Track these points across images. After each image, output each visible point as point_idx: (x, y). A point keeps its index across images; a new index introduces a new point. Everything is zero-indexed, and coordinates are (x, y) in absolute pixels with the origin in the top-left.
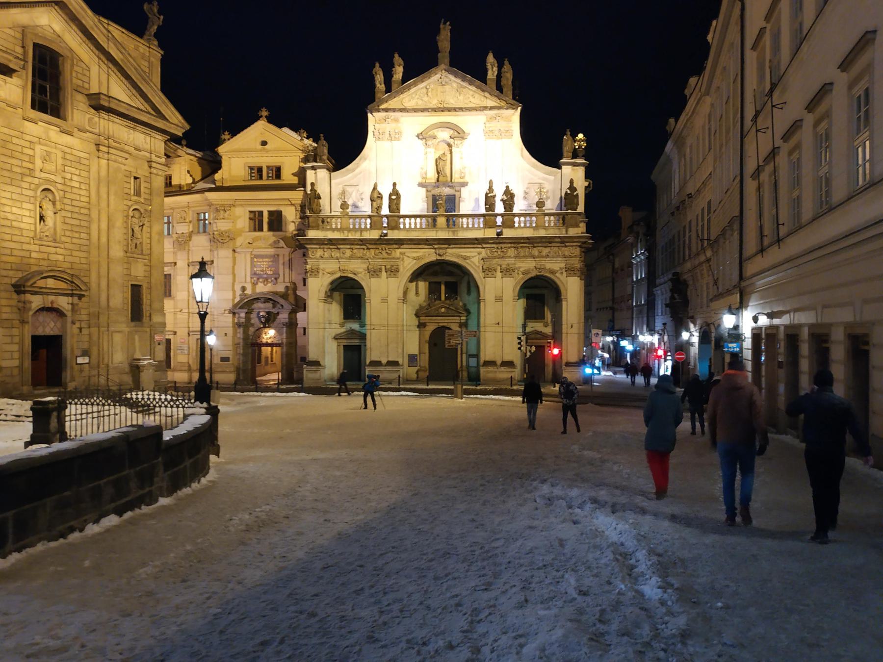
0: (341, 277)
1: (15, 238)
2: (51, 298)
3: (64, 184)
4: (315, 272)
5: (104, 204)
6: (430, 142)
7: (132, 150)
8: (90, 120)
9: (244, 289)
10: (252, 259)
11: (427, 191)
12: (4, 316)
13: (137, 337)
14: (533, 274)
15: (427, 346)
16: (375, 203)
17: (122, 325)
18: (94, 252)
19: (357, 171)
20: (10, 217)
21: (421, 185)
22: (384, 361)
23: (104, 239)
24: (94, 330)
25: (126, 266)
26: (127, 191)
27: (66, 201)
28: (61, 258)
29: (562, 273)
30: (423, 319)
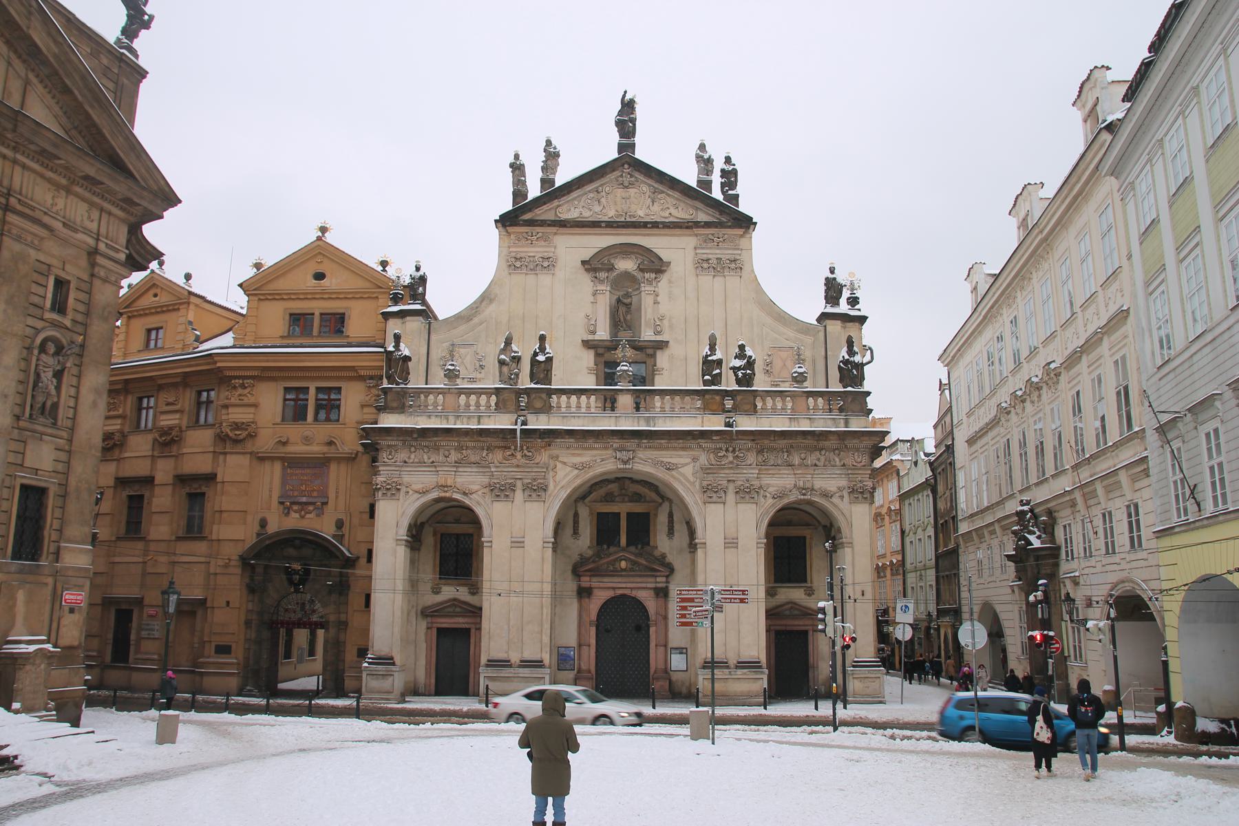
0: (438, 500)
4: (393, 490)
6: (603, 275)
9: (263, 523)
10: (284, 468)
11: (597, 355)
13: (21, 596)
14: (792, 498)
15: (593, 630)
16: (505, 369)
19: (476, 320)
21: (587, 344)
22: (515, 658)
25: (14, 446)
26: (36, 300)
29: (842, 497)
30: (586, 582)
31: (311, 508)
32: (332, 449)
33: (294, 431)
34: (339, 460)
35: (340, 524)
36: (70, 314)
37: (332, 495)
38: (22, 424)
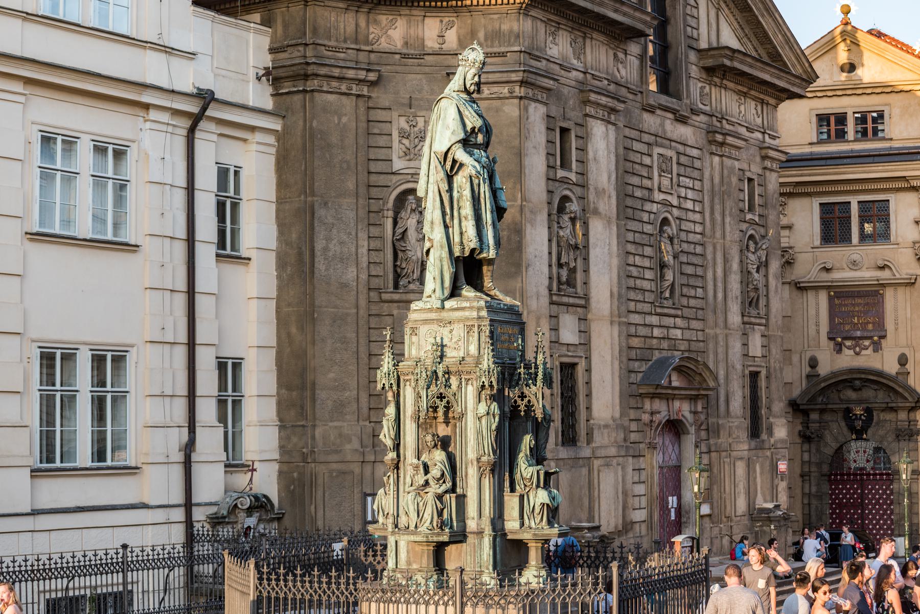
1: (640, 307)
2: (677, 404)
3: (679, 208)
5: (718, 234)
7: (743, 131)
8: (702, 88)
10: (831, 299)
12: (633, 437)
17: (743, 447)
18: (710, 318)
20: (634, 271)
23: (720, 295)
24: (713, 455)
26: (741, 205)
27: (683, 236)
28: (678, 333)
31: (867, 343)
32: (886, 274)
33: (836, 254)
34: (896, 285)
35: (903, 360)
36: (758, 210)
37: (889, 326)
38: (746, 319)
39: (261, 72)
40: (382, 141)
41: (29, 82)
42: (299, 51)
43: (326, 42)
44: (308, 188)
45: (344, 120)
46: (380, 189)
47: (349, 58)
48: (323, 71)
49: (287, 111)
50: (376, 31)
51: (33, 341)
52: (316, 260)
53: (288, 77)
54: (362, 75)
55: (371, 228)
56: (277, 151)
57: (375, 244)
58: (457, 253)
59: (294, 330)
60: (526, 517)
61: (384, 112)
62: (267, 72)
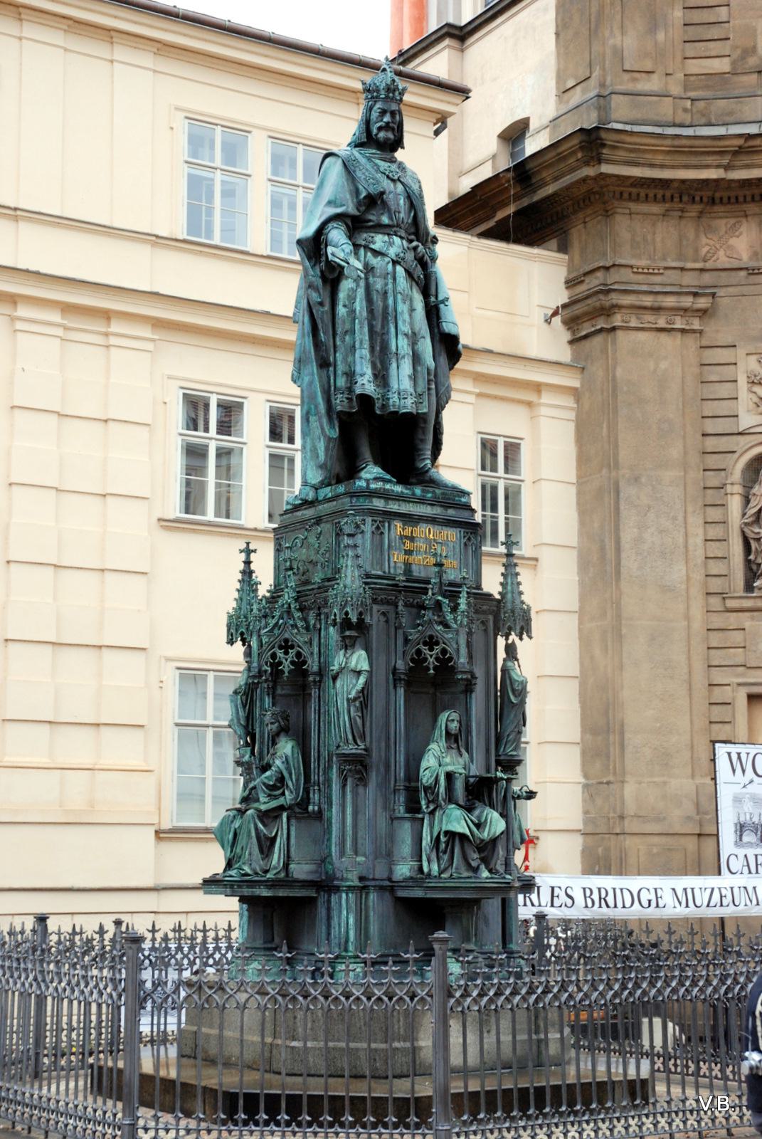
39: (550, 312)
40: (724, 390)
41: (159, 324)
42: (596, 278)
43: (633, 262)
44: (612, 462)
45: (663, 365)
46: (721, 455)
47: (669, 282)
48: (627, 300)
49: (586, 360)
50: (711, 242)
51: (168, 659)
52: (623, 555)
53: (587, 316)
54: (687, 301)
55: (709, 510)
56: (577, 416)
57: (714, 532)
58: (340, 403)
59: (597, 652)
60: (424, 858)
61: (725, 351)
62: (555, 313)
